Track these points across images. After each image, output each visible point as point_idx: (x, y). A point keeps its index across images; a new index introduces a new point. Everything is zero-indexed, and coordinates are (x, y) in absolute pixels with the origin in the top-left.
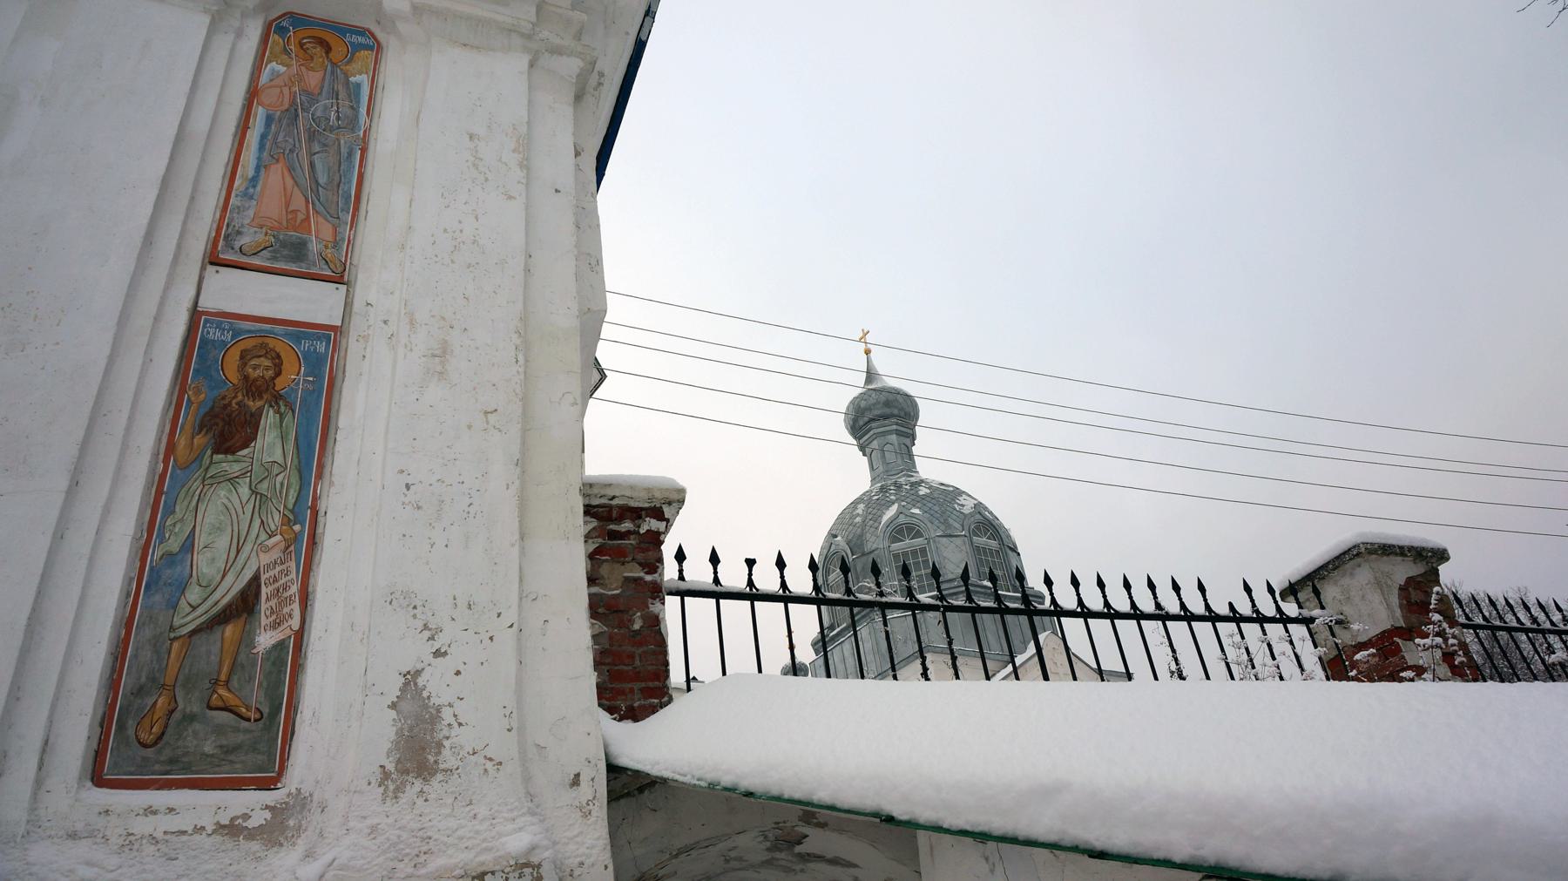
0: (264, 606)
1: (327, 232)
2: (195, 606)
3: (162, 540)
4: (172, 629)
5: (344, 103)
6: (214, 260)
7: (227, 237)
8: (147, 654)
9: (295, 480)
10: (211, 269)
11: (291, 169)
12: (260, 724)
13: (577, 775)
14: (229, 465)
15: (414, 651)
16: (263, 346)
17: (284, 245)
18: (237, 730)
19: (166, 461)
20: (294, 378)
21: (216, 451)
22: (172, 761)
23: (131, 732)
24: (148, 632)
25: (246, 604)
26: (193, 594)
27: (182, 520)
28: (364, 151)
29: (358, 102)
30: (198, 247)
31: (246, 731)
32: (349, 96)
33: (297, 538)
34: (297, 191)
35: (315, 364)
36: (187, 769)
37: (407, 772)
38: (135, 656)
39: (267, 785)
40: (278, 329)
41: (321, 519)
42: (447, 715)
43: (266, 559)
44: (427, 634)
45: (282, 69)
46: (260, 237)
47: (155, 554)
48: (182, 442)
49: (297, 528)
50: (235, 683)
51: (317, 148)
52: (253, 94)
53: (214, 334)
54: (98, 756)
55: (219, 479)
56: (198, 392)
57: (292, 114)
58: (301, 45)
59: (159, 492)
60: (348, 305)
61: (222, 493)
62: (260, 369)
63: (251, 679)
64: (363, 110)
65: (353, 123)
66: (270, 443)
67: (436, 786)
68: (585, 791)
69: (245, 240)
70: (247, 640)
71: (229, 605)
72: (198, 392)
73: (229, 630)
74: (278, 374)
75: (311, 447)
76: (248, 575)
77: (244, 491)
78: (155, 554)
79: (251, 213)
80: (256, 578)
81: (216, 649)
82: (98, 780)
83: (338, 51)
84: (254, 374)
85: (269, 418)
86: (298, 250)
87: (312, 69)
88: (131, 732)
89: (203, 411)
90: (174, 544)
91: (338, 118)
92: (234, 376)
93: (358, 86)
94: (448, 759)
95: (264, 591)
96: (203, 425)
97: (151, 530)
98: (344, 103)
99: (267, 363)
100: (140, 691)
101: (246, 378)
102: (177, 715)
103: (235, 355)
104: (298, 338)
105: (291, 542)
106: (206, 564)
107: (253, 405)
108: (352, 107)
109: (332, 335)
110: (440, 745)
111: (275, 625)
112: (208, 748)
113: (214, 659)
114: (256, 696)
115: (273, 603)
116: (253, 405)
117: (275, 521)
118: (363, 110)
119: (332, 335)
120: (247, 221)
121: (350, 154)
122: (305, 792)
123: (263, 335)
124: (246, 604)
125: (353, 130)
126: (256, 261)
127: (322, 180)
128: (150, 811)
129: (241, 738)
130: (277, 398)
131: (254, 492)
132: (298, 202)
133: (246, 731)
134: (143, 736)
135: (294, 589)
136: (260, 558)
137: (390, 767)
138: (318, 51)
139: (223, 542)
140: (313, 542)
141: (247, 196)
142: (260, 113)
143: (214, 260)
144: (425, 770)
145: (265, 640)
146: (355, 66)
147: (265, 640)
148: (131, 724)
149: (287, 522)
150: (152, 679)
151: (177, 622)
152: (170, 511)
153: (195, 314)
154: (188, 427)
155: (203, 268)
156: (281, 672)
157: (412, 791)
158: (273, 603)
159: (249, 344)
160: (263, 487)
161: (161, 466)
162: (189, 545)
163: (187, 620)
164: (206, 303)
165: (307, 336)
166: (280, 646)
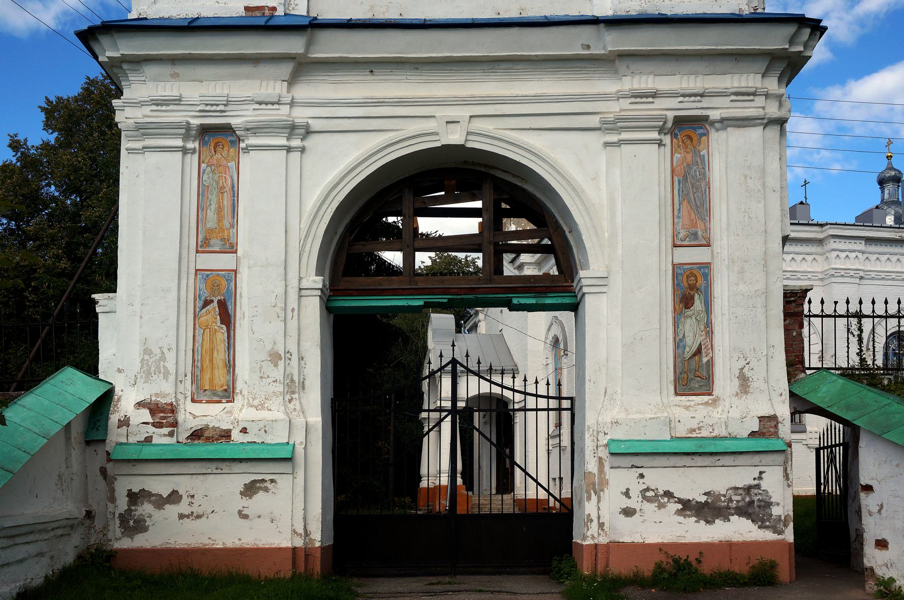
0: (703, 351)
2: (688, 354)
3: (678, 335)
4: (685, 358)
5: (701, 166)
6: (675, 246)
7: (676, 235)
8: (680, 364)
9: (705, 315)
10: (675, 248)
11: (689, 202)
12: (707, 380)
13: (782, 393)
14: (689, 312)
15: (742, 363)
16: (692, 273)
17: (692, 234)
18: (702, 382)
19: (674, 313)
20: (701, 282)
21: (686, 309)
22: (690, 389)
23: (681, 383)
24: (680, 360)
26: (687, 349)
27: (681, 330)
28: (709, 188)
29: (705, 164)
30: (670, 240)
31: (704, 382)
32: (701, 162)
33: (708, 331)
34: (692, 211)
35: (707, 277)
36: (693, 390)
37: (742, 393)
38: (678, 365)
39: (710, 394)
40: (695, 266)
41: (713, 326)
42: (750, 379)
43: (702, 338)
44: (744, 359)
45: (679, 156)
46: (685, 233)
47: (677, 339)
48: (677, 307)
49: (708, 329)
50: (700, 371)
51: (695, 191)
52: (673, 171)
53: (679, 271)
54: (675, 388)
55: (686, 317)
56: (678, 291)
57: (685, 178)
58: (683, 141)
59: (675, 323)
60: (712, 253)
61: (688, 321)
63: (703, 370)
64: (707, 169)
65: (704, 174)
66: (698, 305)
67: (749, 396)
68: (783, 397)
69: (681, 236)
70: (701, 360)
71: (696, 351)
72: (678, 291)
73: (696, 357)
74: (697, 282)
75: (708, 304)
76: (698, 343)
77: (694, 319)
78: (677, 339)
79: (681, 224)
80: (700, 344)
81: (694, 362)
82: (676, 394)
83: (695, 138)
85: (696, 297)
86: (695, 235)
87: (688, 153)
88: (681, 383)
89: (681, 296)
90: (681, 336)
91: (700, 175)
92: (686, 284)
93: (704, 156)
94: (751, 390)
96: (681, 301)
97: (675, 332)
98: (701, 166)
99: (694, 278)
100: (681, 373)
101: (689, 284)
102: (689, 379)
103: (685, 277)
104: (700, 268)
105: (707, 333)
106: (689, 340)
107: (692, 293)
108: (703, 168)
109: (708, 265)
110: (749, 386)
111: (706, 356)
112: (697, 386)
113: (694, 365)
114: (705, 374)
115: (705, 350)
116: (692, 293)
117: (702, 327)
118: (707, 169)
119: (708, 265)
120: (680, 228)
121: (705, 190)
122: (719, 396)
123: (691, 269)
124: (699, 351)
125: (705, 179)
126: (685, 243)
127: (698, 205)
128: (689, 401)
129: (702, 383)
130: (698, 289)
131: (696, 320)
132: (693, 216)
133: (704, 382)
134: (683, 383)
135: (710, 346)
136: (700, 339)
137: (739, 392)
138: (689, 142)
139: (691, 335)
140: (712, 332)
141: (679, 217)
142: (676, 179)
143: (675, 246)
144: (746, 392)
145: (705, 360)
146: (702, 146)
147: (705, 360)
148: (680, 381)
149: (705, 327)
150: (683, 370)
151: (685, 356)
152: (678, 328)
153: (673, 265)
154: (678, 302)
155: (672, 249)
156: (710, 368)
157: (744, 398)
158: (705, 350)
159: (688, 273)
160: (698, 318)
161: (673, 315)
162: (684, 336)
163: (687, 356)
164: (676, 261)
166: (708, 360)
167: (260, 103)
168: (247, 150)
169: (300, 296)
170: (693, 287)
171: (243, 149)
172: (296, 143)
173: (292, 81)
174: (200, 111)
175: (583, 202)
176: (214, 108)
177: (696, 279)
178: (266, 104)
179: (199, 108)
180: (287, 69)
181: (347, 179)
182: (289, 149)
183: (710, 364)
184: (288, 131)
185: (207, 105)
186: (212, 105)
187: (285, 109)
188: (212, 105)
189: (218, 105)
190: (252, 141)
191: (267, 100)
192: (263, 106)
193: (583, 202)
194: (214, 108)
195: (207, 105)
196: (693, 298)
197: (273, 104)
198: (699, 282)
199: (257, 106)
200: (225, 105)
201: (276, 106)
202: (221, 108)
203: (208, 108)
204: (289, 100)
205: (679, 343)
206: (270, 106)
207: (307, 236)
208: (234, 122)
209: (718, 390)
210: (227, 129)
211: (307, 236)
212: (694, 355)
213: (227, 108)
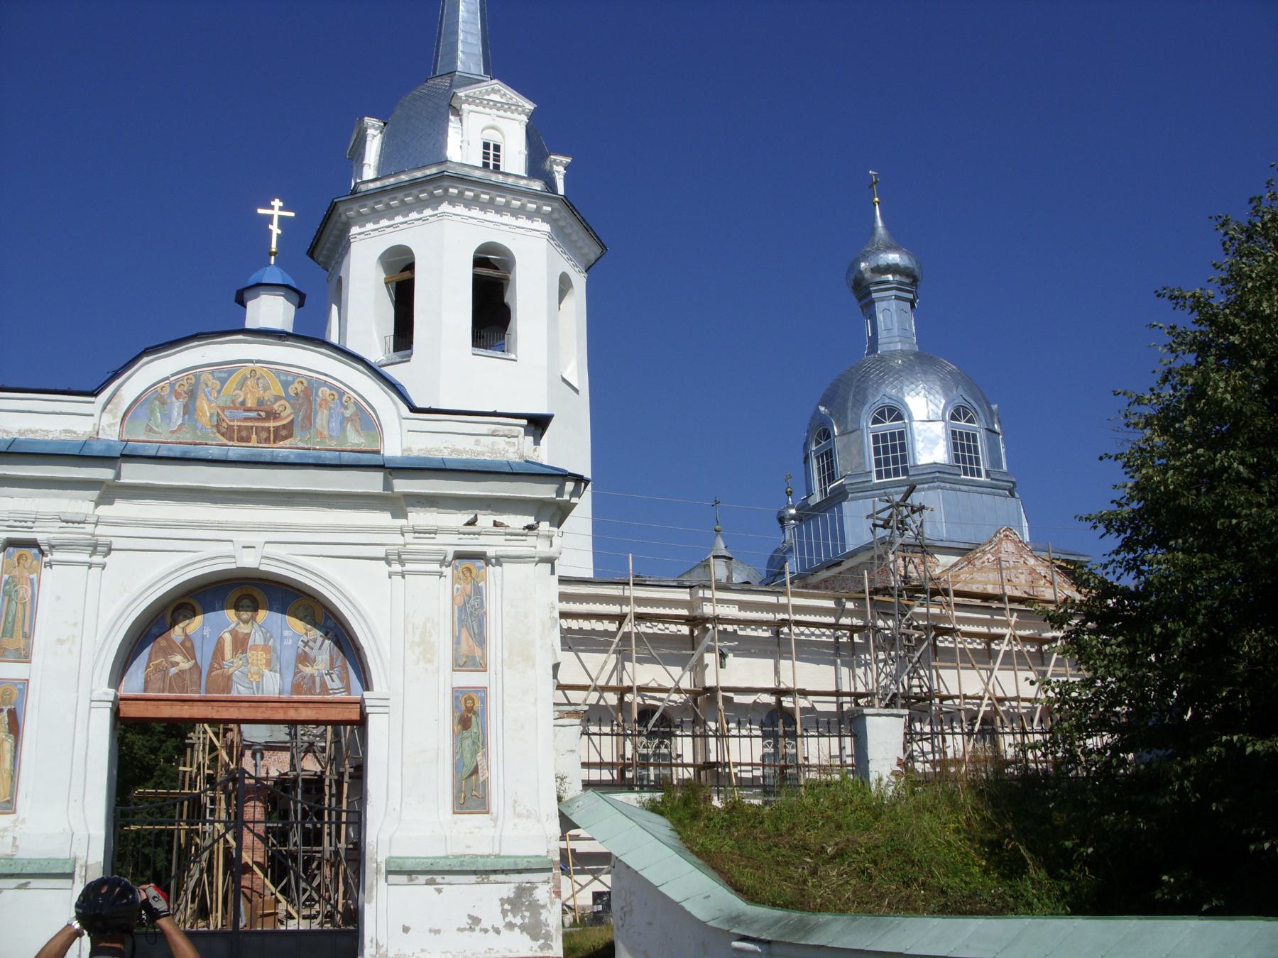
0: (480, 771)
1: (480, 654)
6: (454, 670)
14: (466, 734)
20: (478, 706)
25: (475, 771)
35: (484, 701)
62: (469, 703)
66: (474, 729)
70: (477, 780)
73: (473, 777)
84: (468, 705)
85: (474, 719)
95: (480, 767)
99: (470, 701)
104: (477, 692)
107: (469, 715)
116: (469, 715)
145: (481, 779)
147: (481, 779)
165: (480, 691)
167: (67, 522)
168: (49, 565)
169: (91, 708)
170: (470, 710)
171: (45, 563)
172: (97, 559)
173: (97, 504)
174: (8, 526)
175: (368, 627)
176: (23, 524)
177: (474, 703)
178: (73, 522)
179: (7, 523)
180: (94, 494)
181: (145, 595)
182: (90, 566)
183: (485, 784)
184: (91, 548)
185: (15, 521)
186: (21, 521)
187: (89, 528)
188: (21, 521)
189: (26, 522)
190: (57, 556)
191: (74, 519)
192: (70, 525)
193: (368, 627)
194: (23, 524)
195: (15, 521)
196: (470, 720)
197: (79, 523)
198: (477, 705)
199: (64, 524)
200: (34, 522)
201: (81, 525)
202: (30, 524)
203: (16, 524)
204: (94, 520)
205: (458, 765)
206: (76, 525)
207: (101, 649)
208: (41, 538)
209: (493, 808)
210: (33, 544)
211: (101, 649)
212: (471, 775)
213: (36, 524)
